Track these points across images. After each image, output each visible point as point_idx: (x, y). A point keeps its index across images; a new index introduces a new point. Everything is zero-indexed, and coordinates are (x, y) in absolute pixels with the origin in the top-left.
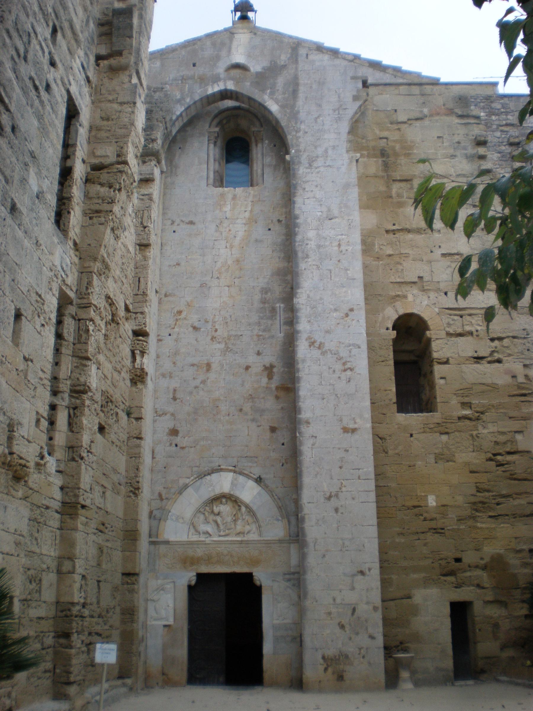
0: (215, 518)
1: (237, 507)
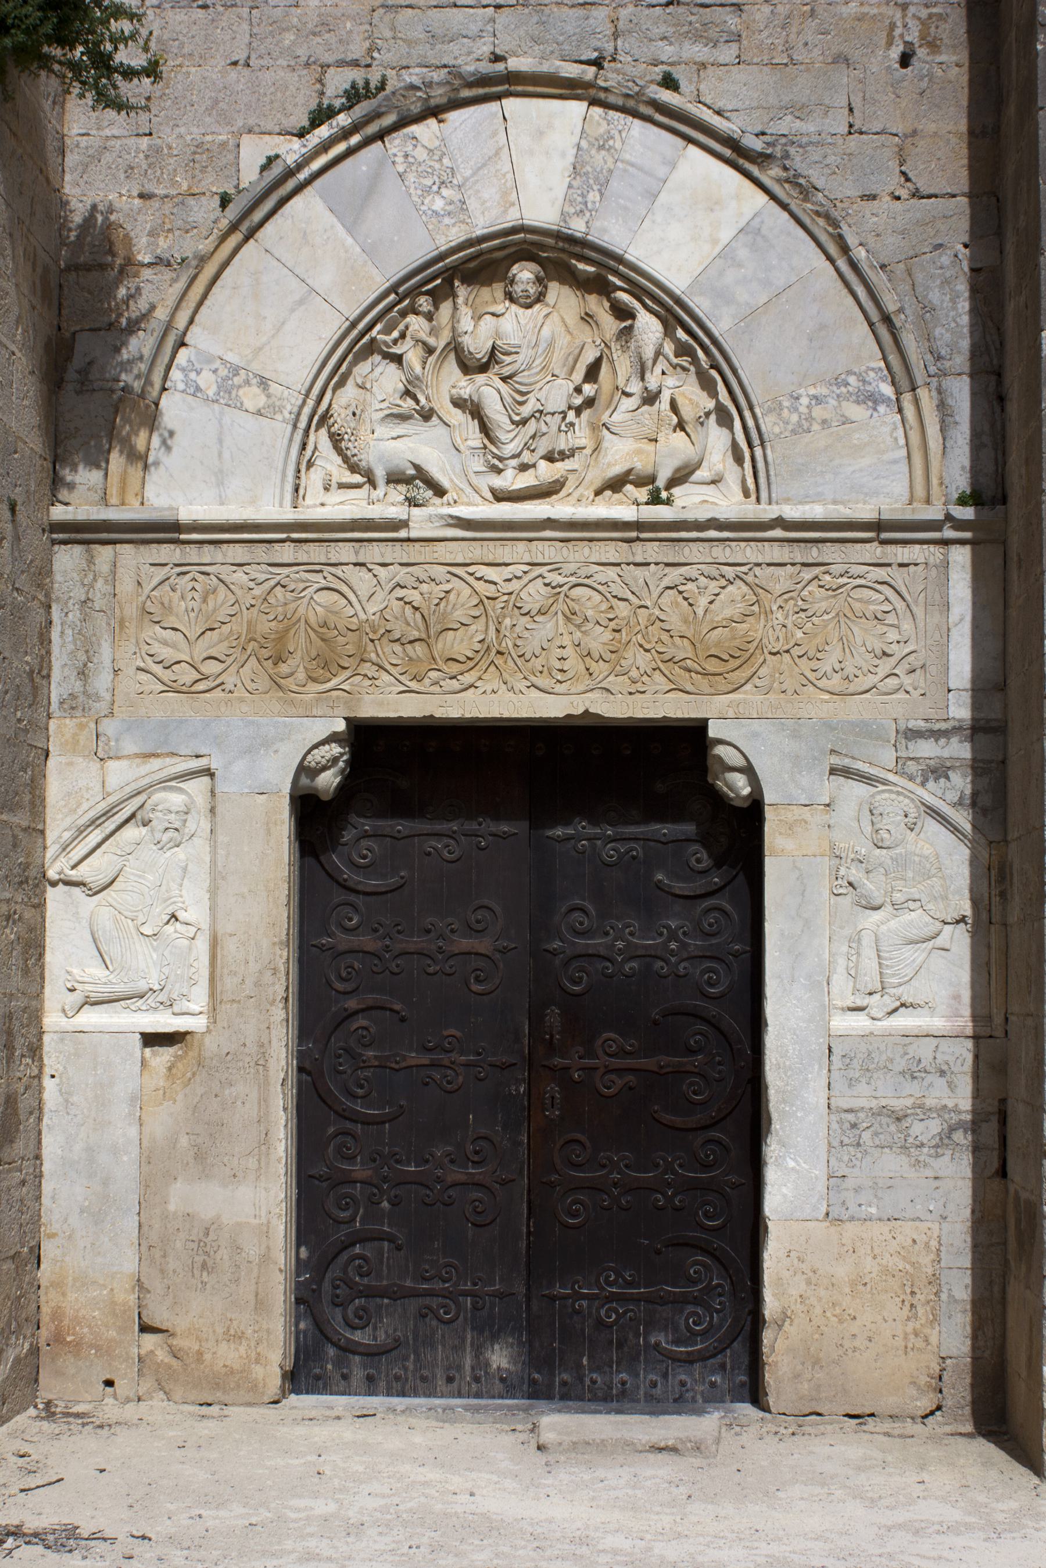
0: (466, 386)
1: (610, 324)
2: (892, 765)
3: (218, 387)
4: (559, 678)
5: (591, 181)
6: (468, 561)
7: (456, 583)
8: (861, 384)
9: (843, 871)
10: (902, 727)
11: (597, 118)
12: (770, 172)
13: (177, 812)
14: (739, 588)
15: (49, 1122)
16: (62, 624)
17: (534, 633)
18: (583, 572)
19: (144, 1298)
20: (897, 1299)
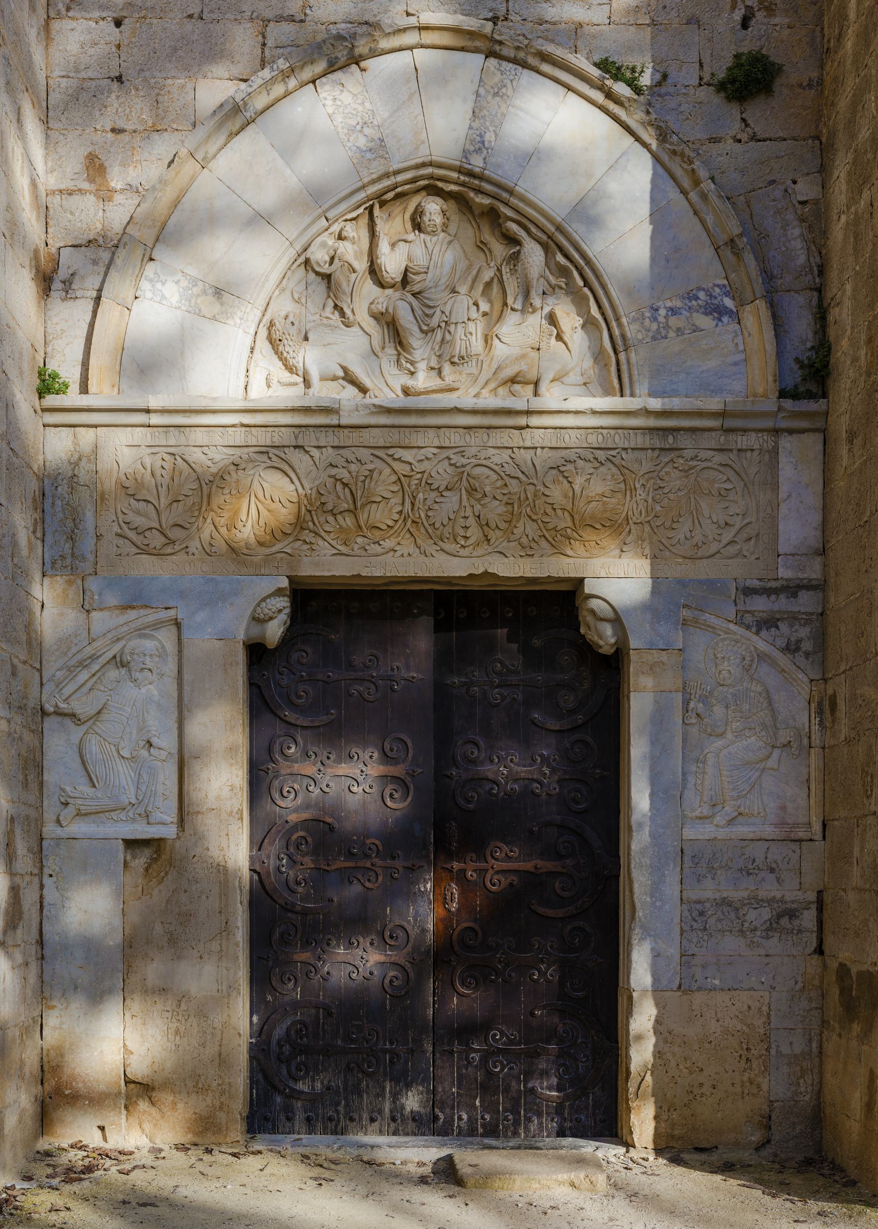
2: (732, 617)
3: (181, 296)
4: (463, 543)
5: (488, 124)
6: (388, 445)
7: (378, 464)
8: (708, 298)
9: (692, 705)
10: (741, 585)
11: (492, 68)
12: (634, 116)
13: (151, 655)
14: (609, 469)
15: (48, 914)
16: (53, 496)
17: (443, 505)
18: (483, 455)
19: (128, 1058)
20: (736, 1054)
